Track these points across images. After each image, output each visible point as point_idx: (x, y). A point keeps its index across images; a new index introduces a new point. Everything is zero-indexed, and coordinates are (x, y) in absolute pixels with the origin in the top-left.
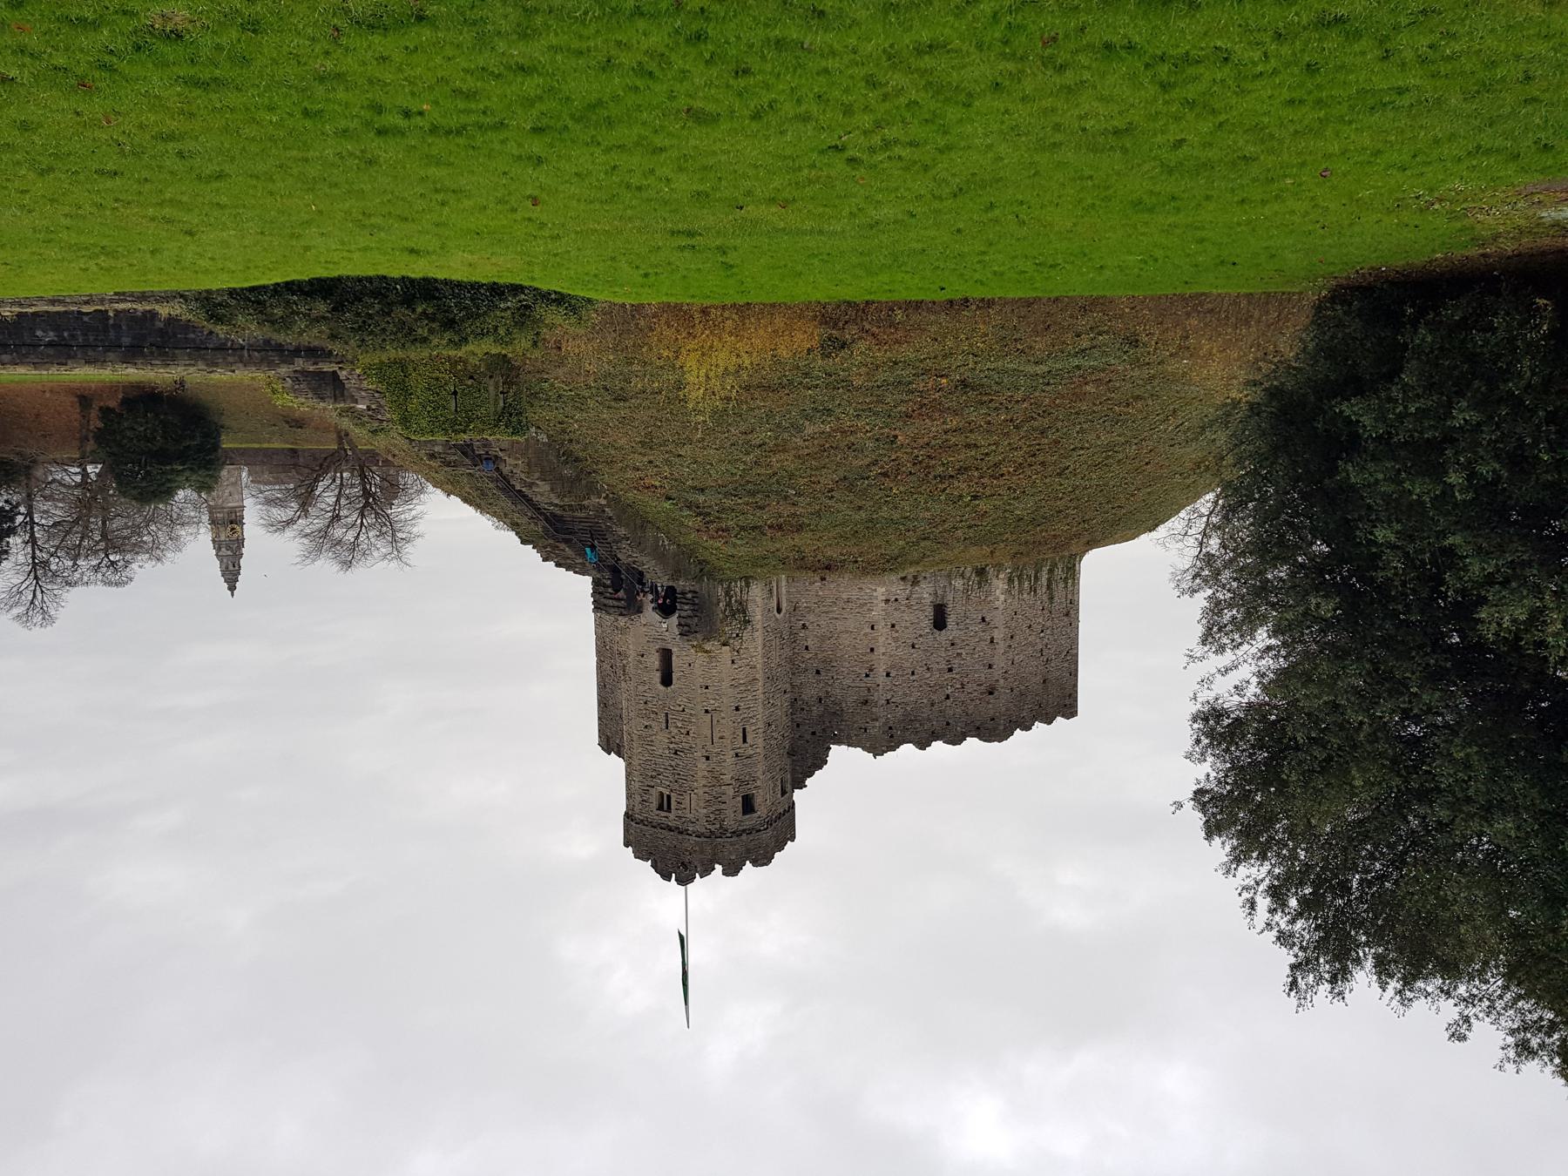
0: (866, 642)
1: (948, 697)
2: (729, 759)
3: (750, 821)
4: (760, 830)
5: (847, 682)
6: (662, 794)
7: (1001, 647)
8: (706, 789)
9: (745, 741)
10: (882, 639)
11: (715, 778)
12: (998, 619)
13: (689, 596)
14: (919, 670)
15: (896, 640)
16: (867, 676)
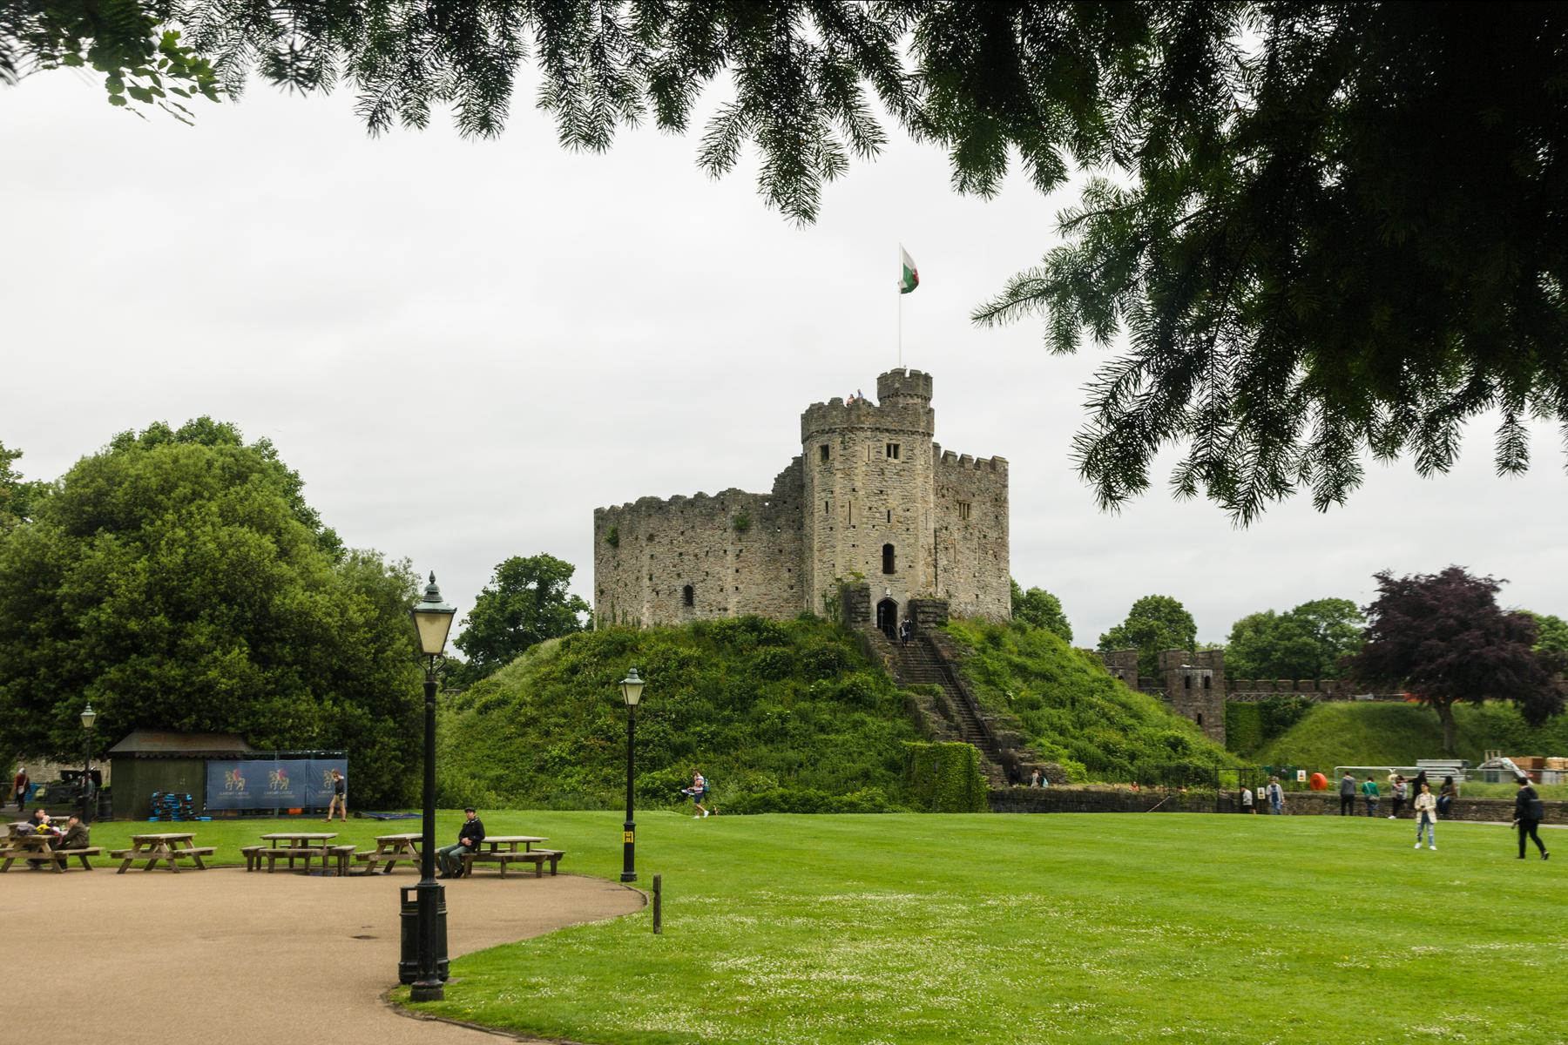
0: (742, 577)
1: (682, 533)
2: (837, 489)
3: (823, 440)
4: (817, 432)
5: (756, 545)
6: (896, 457)
7: (645, 572)
8: (855, 465)
9: (827, 503)
10: (729, 580)
11: (848, 474)
12: (647, 594)
13: (859, 619)
14: (702, 555)
15: (720, 579)
16: (741, 551)
